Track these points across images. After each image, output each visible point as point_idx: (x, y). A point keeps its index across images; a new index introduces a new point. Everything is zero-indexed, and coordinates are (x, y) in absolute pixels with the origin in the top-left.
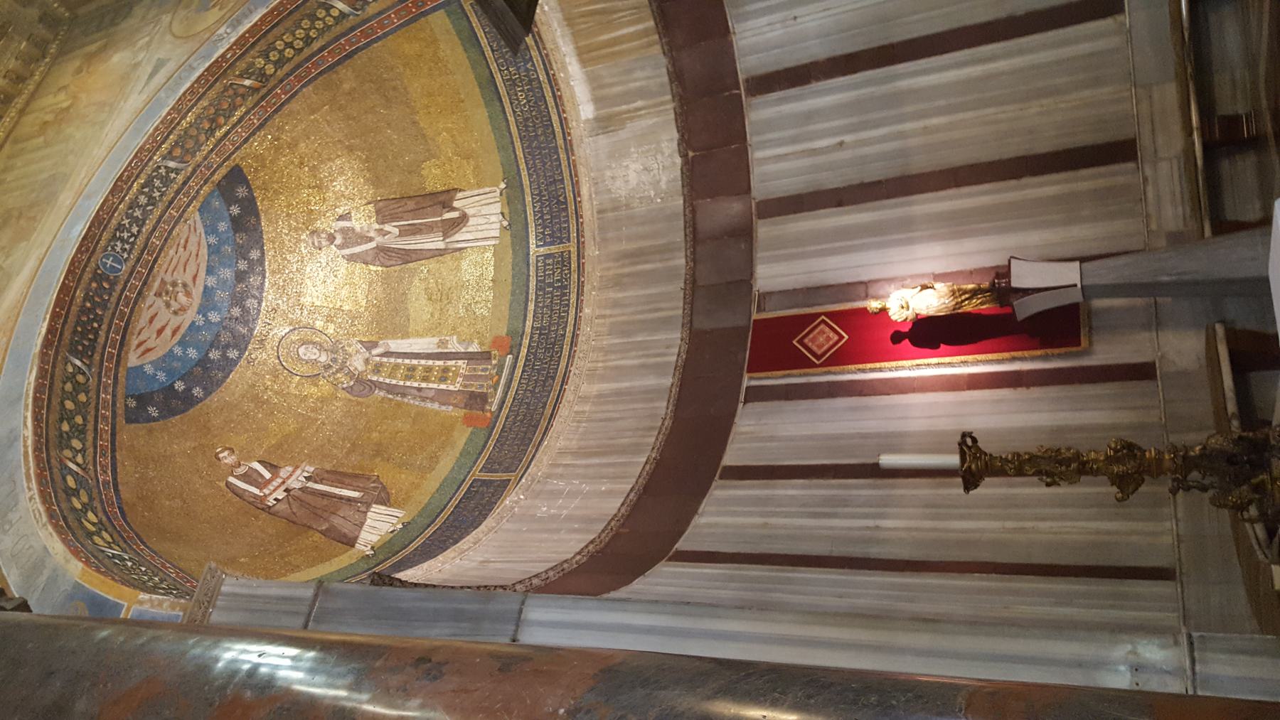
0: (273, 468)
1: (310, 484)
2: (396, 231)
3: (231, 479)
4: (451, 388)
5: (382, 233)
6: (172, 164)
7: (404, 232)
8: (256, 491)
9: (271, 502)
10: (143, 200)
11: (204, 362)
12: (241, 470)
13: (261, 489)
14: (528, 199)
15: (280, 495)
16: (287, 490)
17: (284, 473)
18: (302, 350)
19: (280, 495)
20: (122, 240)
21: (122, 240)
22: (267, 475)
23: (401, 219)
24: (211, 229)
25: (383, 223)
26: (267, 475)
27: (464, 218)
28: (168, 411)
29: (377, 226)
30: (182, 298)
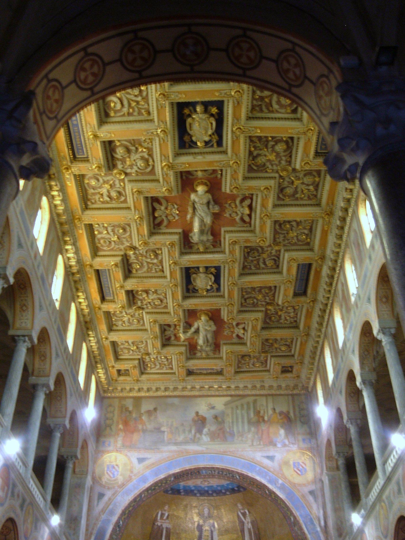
2: (249, 527)
5: (248, 523)
6: (238, 477)
7: (249, 530)
9: (156, 524)
10: (225, 473)
11: (192, 491)
12: (164, 512)
16: (161, 525)
17: (167, 521)
20: (212, 472)
21: (212, 472)
23: (253, 528)
24: (227, 484)
25: (251, 523)
26: (165, 518)
28: (173, 493)
29: (249, 521)
30: (206, 483)
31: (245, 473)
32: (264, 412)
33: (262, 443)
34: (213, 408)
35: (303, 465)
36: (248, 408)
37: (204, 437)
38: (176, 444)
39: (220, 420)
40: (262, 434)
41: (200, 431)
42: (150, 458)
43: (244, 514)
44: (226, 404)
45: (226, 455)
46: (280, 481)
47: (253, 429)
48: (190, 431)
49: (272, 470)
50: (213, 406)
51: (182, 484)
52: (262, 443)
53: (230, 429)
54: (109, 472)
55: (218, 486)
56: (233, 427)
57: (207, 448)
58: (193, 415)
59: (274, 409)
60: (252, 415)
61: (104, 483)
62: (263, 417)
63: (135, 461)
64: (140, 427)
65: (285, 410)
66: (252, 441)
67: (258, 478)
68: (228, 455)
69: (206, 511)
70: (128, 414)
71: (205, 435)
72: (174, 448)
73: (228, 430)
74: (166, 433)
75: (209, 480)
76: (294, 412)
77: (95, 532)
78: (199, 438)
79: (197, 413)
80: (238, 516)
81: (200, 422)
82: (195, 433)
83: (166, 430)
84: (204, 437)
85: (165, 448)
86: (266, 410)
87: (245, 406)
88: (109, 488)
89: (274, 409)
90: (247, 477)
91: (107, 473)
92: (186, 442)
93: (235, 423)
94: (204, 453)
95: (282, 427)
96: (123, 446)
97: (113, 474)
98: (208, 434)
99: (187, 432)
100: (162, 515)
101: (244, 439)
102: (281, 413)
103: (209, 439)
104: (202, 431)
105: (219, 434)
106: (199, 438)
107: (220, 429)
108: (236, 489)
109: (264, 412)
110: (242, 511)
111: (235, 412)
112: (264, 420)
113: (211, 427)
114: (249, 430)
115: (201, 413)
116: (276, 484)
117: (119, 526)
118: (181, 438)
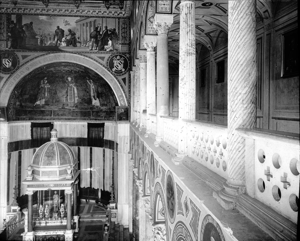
1: (46, 88)
3: (42, 81)
4: (69, 100)
8: (42, 83)
13: (43, 84)
15: (43, 86)
22: (45, 83)
26: (45, 83)
27: (95, 99)
34: (69, 24)
36: (91, 26)
37: (62, 42)
44: (77, 22)
50: (69, 22)
52: (97, 49)
66: (92, 48)
71: (63, 42)
76: (119, 29)
78: (59, 44)
79: (58, 27)
83: (39, 37)
86: (101, 27)
87: (89, 24)
98: (65, 41)
99: (52, 40)
106: (59, 44)
107: (73, 39)
111: (82, 27)
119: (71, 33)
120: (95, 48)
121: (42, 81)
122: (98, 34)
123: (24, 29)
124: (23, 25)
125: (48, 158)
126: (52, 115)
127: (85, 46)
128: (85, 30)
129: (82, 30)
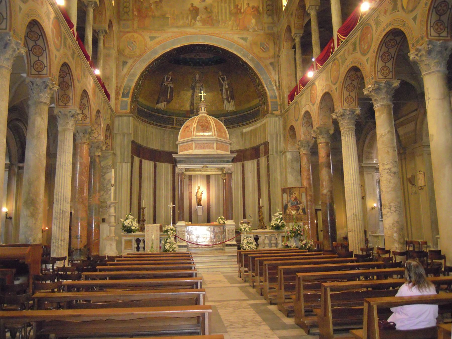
0: (171, 80)
1: (169, 88)
2: (226, 87)
3: (166, 76)
5: (226, 84)
6: (221, 52)
9: (164, 84)
10: (212, 49)
12: (168, 76)
14: (233, 116)
15: (166, 85)
16: (167, 85)
17: (170, 82)
18: (197, 75)
19: (166, 85)
21: (203, 48)
22: (169, 80)
23: (229, 87)
24: (213, 58)
26: (169, 80)
27: (229, 102)
31: (227, 49)
32: (241, 6)
33: (239, 29)
35: (267, 45)
37: (197, 22)
38: (177, 27)
39: (209, 10)
40: (239, 22)
41: (194, 18)
42: (159, 37)
43: (223, 79)
45: (213, 36)
46: (251, 56)
47: (233, 18)
48: (187, 18)
49: (245, 47)
51: (182, 56)
52: (239, 29)
53: (216, 17)
54: (129, 46)
55: (207, 58)
56: (219, 16)
57: (200, 31)
58: (189, 6)
59: (248, 4)
60: (232, 8)
61: (126, 54)
62: (240, 10)
63: (148, 40)
64: (150, 14)
65: (256, 5)
66: (232, 27)
67: (235, 53)
68: (215, 36)
69: (197, 76)
70: (140, 3)
71: (198, 21)
72: (176, 30)
73: (215, 18)
74: (170, 18)
75: (200, 54)
77: (122, 88)
79: (192, 5)
80: (219, 80)
81: (194, 11)
82: (191, 19)
84: (197, 22)
85: (170, 30)
86: (242, 4)
88: (130, 58)
89: (248, 4)
90: (228, 51)
91: (128, 47)
92: (184, 26)
93: (220, 13)
94: (198, 34)
95: (253, 18)
96: (138, 28)
97: (132, 48)
100: (168, 78)
101: (226, 25)
102: (253, 7)
103: (201, 24)
104: (196, 18)
105: (208, 21)
106: (194, 23)
107: (210, 17)
108: (219, 60)
109: (241, 6)
110: (222, 77)
111: (220, 4)
112: (241, 12)
113: (202, 15)
114: (230, 19)
115: (195, 5)
116: (247, 57)
117: (139, 84)
118: (181, 23)
119: (207, 11)
120: (236, 28)
121: (166, 76)
122: (238, 12)
123: (152, 7)
124: (151, 2)
125: (202, 128)
126: (175, 125)
127: (224, 26)
128: (223, 8)
129: (220, 8)
